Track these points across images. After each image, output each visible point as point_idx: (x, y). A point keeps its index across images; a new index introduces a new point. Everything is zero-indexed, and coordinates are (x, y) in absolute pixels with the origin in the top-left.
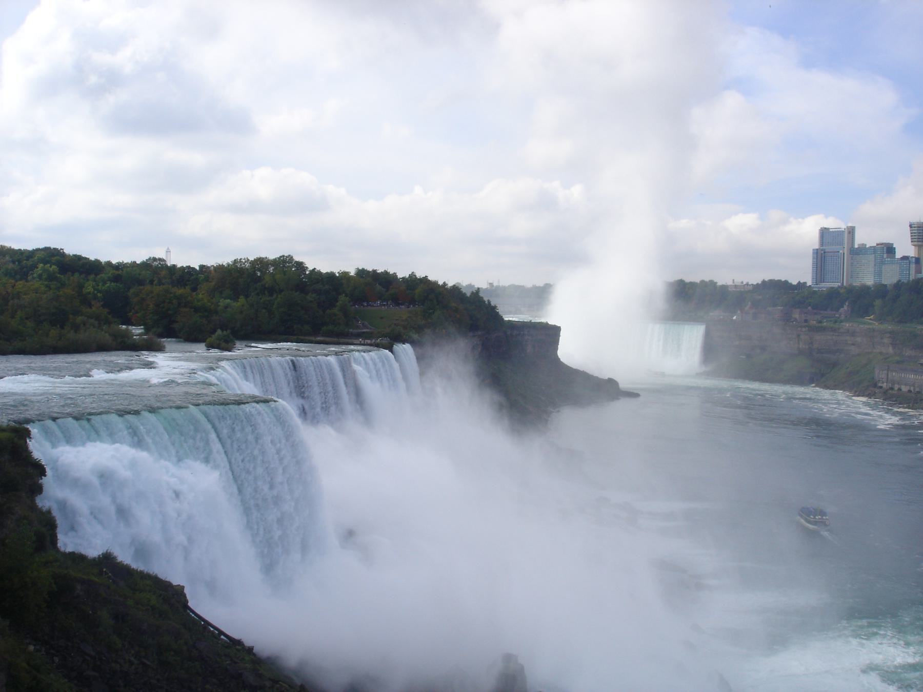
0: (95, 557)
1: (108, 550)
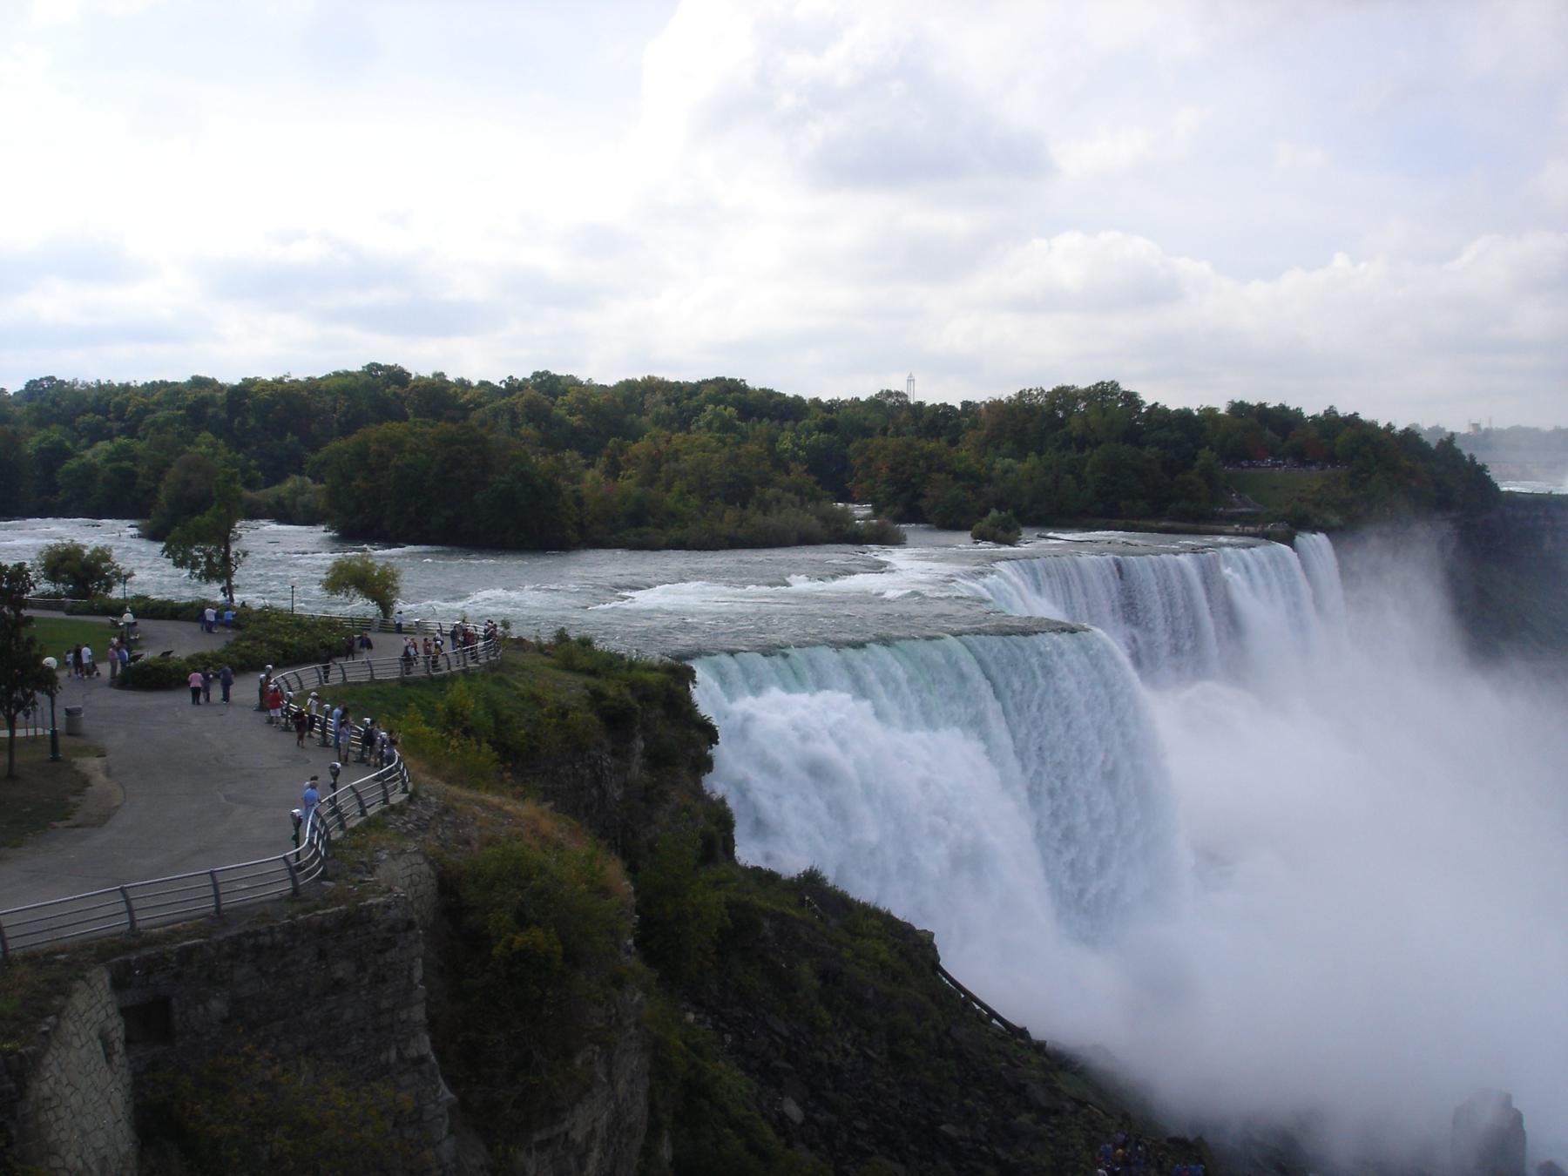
0: (793, 878)
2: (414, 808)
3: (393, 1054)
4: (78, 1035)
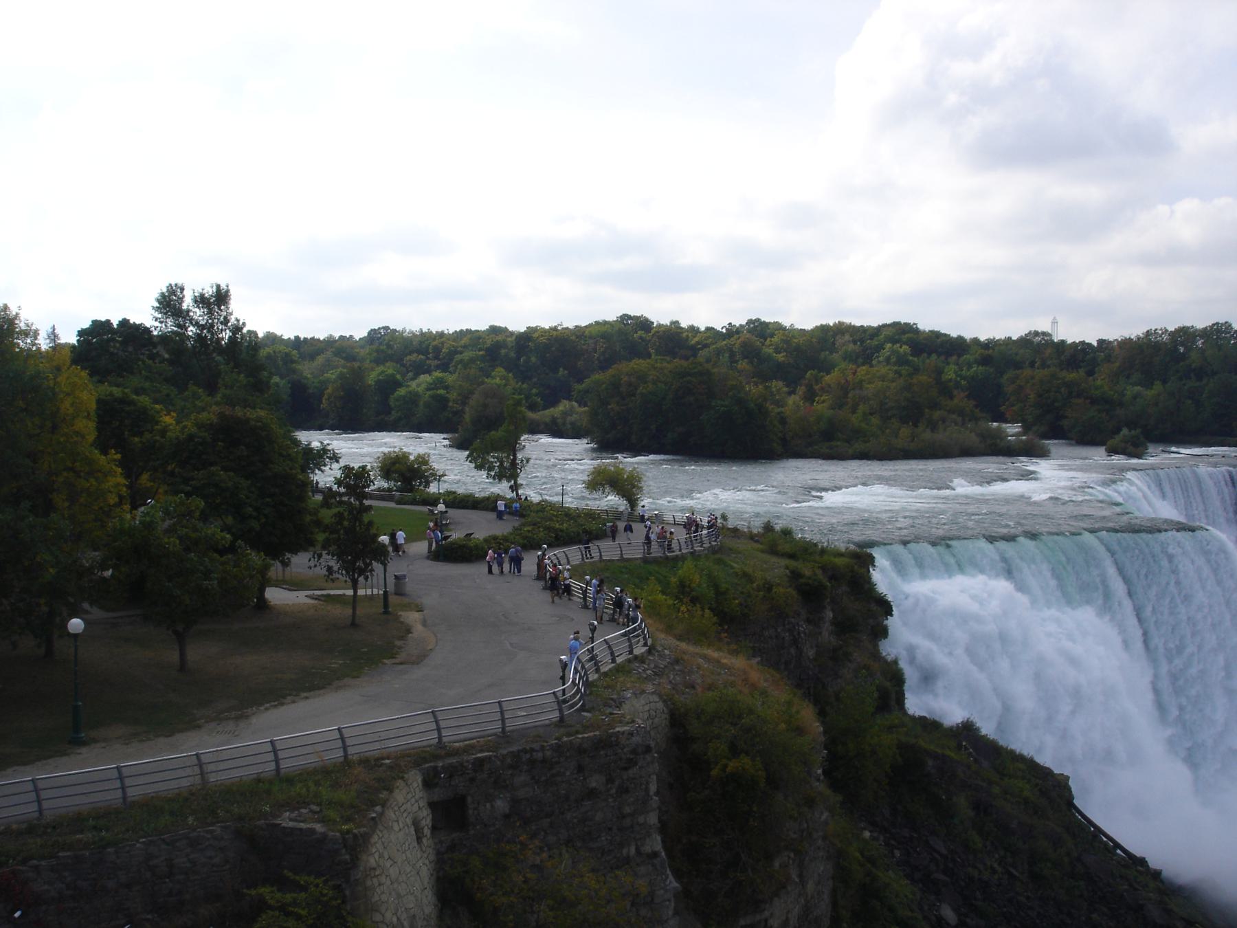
1: (969, 718)
2: (652, 658)
3: (633, 850)
4: (397, 821)
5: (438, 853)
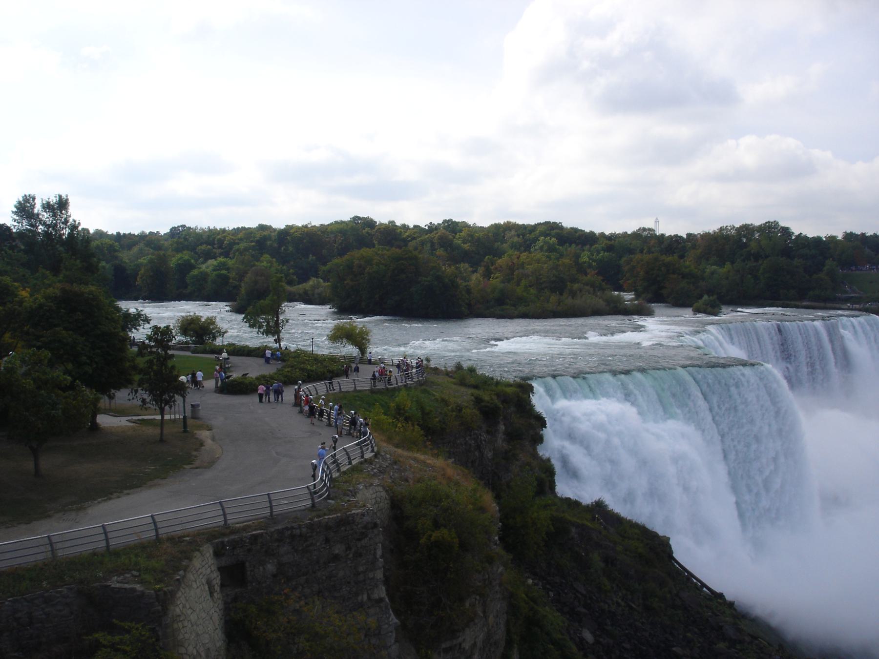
0: (589, 505)
2: (377, 461)
3: (365, 597)
4: (196, 581)
5: (226, 603)
